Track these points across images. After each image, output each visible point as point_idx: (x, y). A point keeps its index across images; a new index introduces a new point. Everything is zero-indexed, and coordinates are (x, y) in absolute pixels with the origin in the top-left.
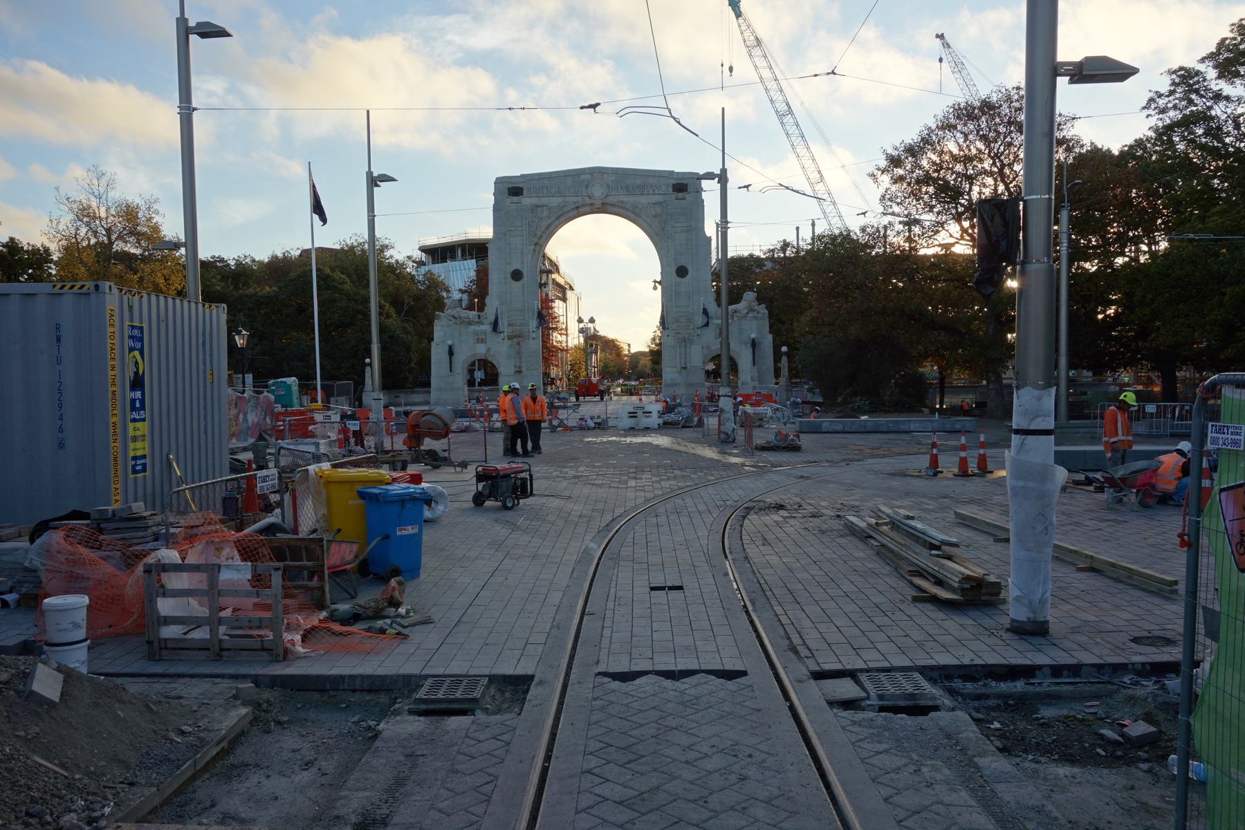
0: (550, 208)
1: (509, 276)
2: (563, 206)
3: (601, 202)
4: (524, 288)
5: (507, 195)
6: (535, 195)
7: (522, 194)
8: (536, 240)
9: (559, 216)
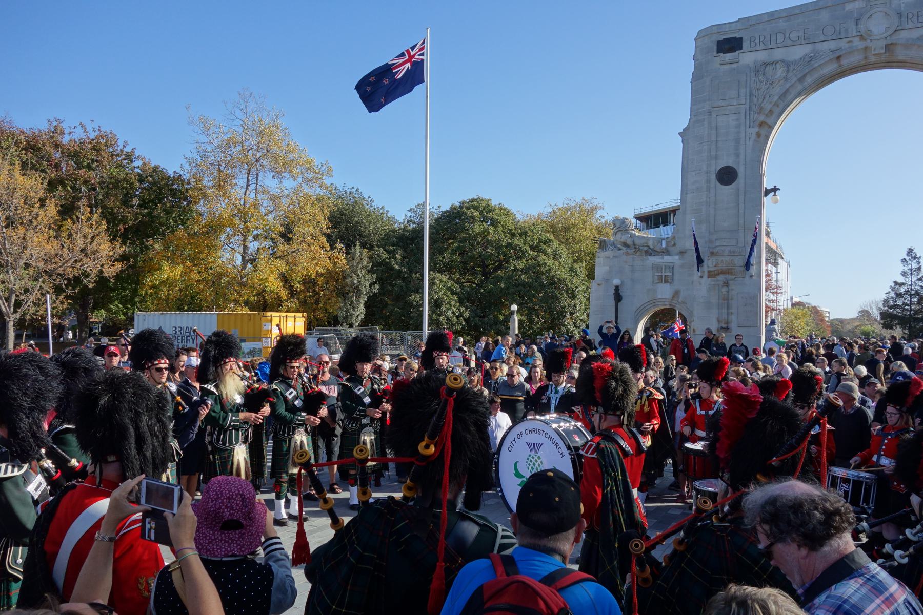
0: (787, 64)
1: (713, 177)
2: (811, 59)
3: (884, 43)
4: (738, 195)
5: (715, 54)
6: (762, 47)
7: (741, 49)
8: (762, 118)
9: (805, 76)
